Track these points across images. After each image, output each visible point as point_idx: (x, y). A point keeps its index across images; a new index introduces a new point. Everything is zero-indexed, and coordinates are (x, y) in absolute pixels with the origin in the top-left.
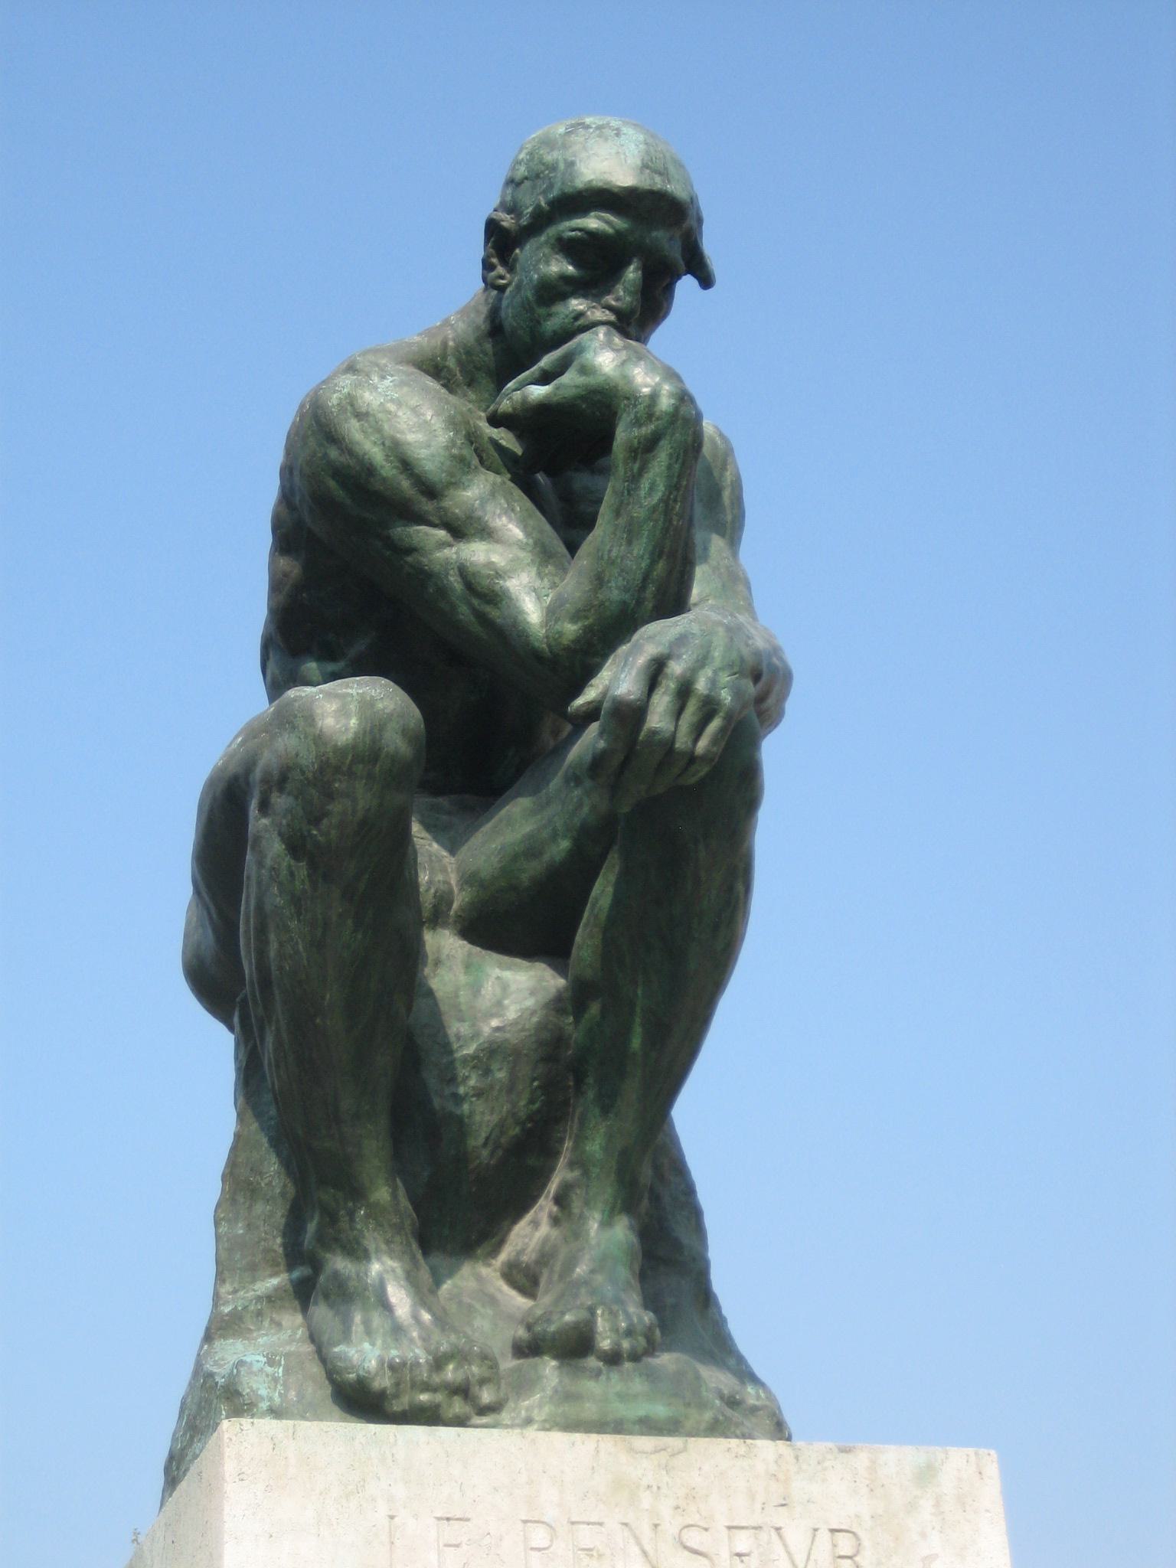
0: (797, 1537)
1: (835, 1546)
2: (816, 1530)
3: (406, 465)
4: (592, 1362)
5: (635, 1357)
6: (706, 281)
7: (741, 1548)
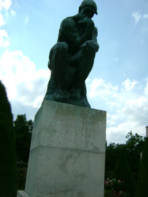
0: (90, 115)
6: (97, 14)
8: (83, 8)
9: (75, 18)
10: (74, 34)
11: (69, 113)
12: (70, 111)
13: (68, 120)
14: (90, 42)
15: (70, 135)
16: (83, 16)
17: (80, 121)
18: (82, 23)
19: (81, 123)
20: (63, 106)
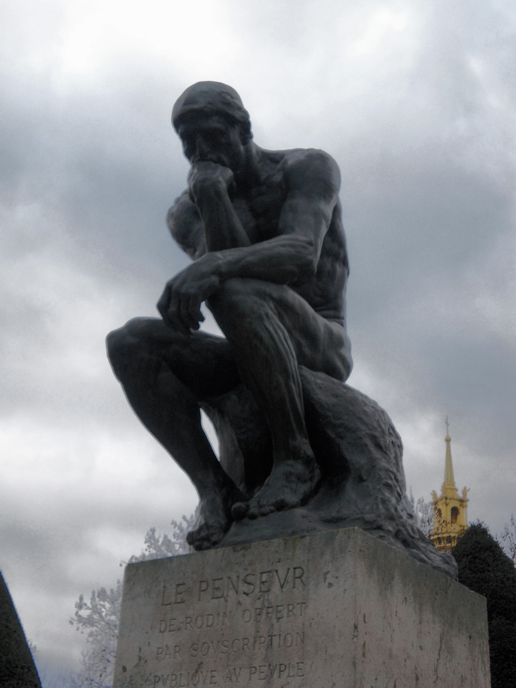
0: (282, 573)
2: (289, 569)
4: (246, 520)
5: (263, 515)
7: (264, 579)
11: (204, 586)
15: (208, 681)
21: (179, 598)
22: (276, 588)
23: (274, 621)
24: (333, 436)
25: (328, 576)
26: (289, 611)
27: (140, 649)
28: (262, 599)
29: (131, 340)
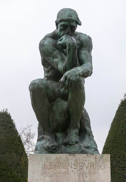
0: (87, 164)
1: (91, 165)
2: (89, 163)
3: (48, 51)
6: (80, 25)
7: (81, 165)
8: (59, 23)
9: (55, 36)
10: (55, 60)
11: (59, 164)
12: (61, 162)
13: (59, 174)
14: (69, 74)
16: (62, 34)
17: (74, 173)
18: (60, 44)
19: (76, 175)
20: (51, 158)
21: (51, 167)
22: (85, 168)
23: (85, 177)
24: (83, 122)
25: (102, 167)
26: (89, 175)
27: (37, 181)
28: (80, 170)
29: (41, 86)
